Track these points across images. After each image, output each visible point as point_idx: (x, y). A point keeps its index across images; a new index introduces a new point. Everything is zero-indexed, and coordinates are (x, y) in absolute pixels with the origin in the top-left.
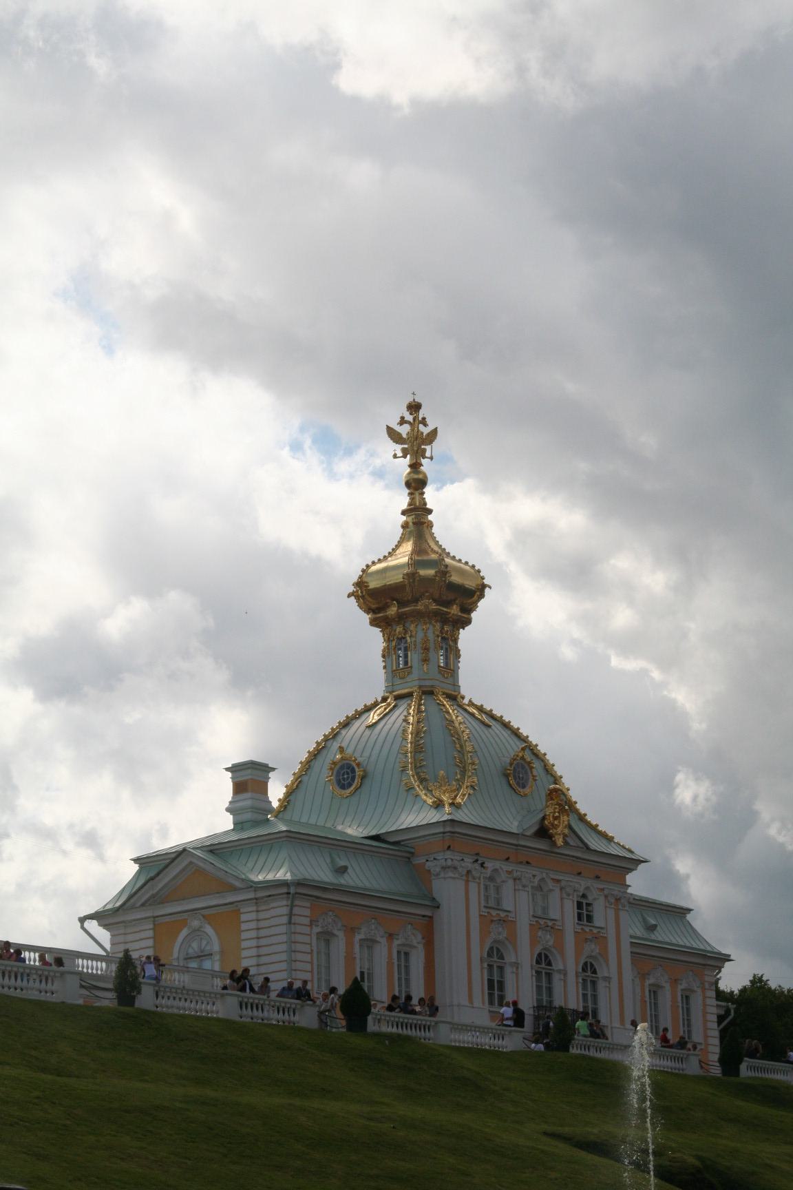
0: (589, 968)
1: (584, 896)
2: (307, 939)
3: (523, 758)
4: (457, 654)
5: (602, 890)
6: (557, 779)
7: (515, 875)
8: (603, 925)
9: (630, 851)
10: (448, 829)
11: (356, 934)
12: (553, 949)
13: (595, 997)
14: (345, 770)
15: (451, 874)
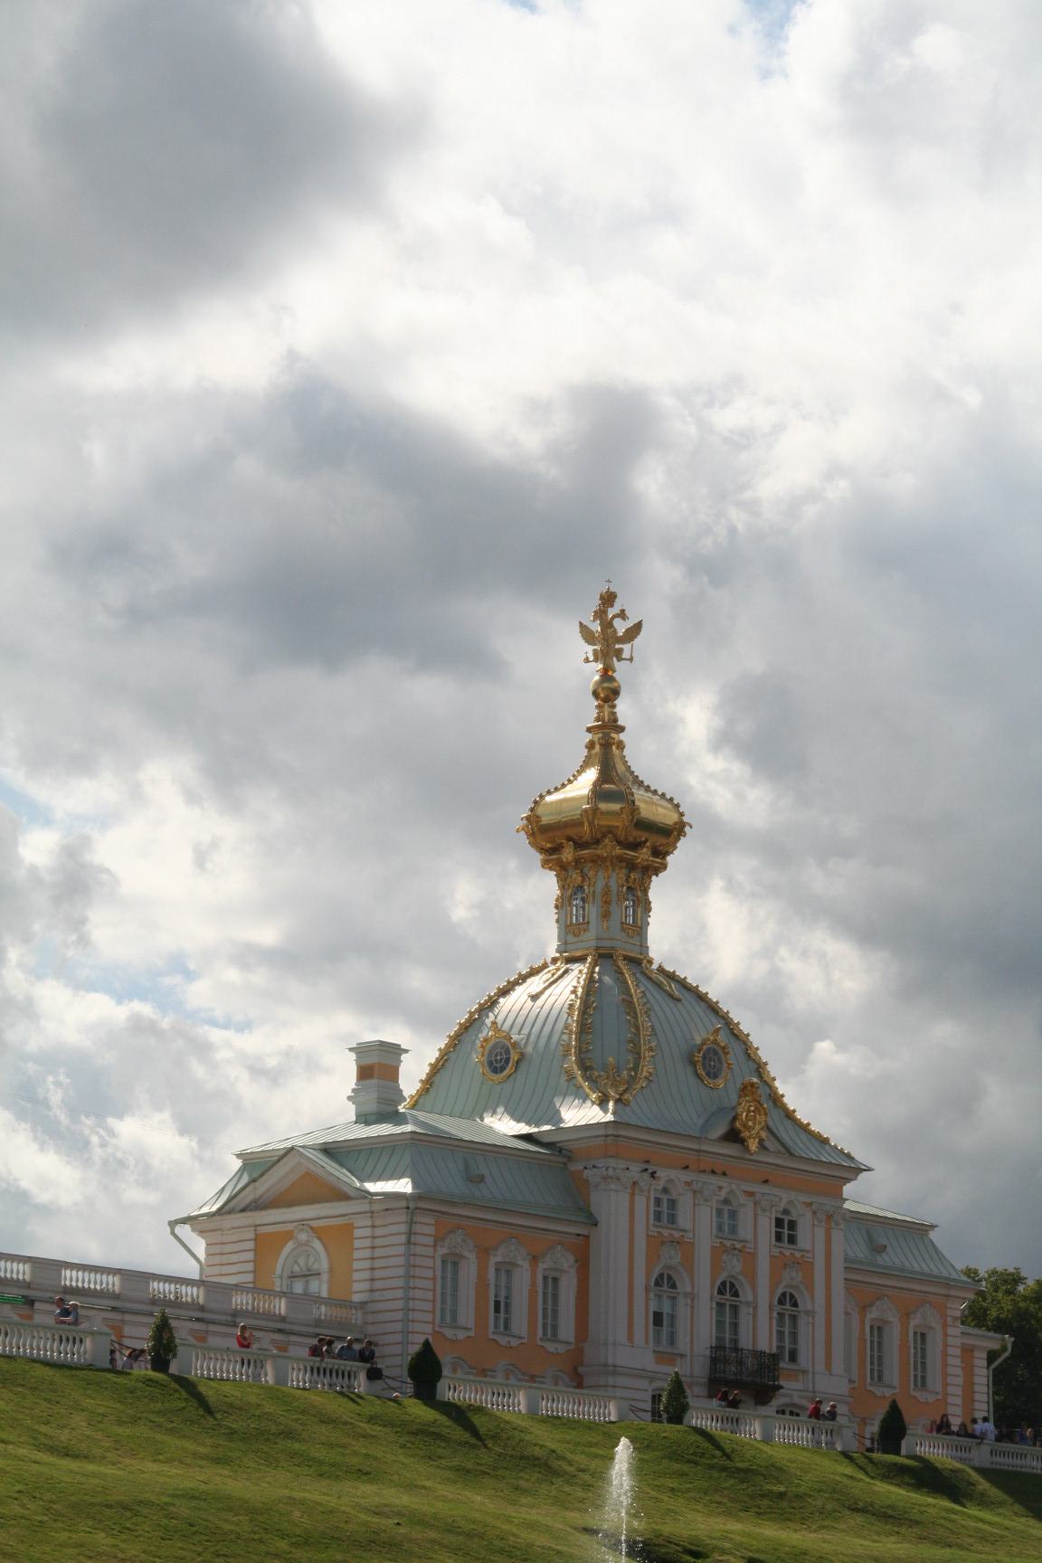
0: (788, 1299)
1: (786, 1212)
2: (429, 1262)
3: (715, 1042)
4: (647, 907)
5: (810, 1204)
6: (760, 1068)
7: (695, 1186)
8: (808, 1247)
9: (848, 1156)
10: (610, 1132)
11: (491, 1257)
12: (741, 1277)
13: (794, 1336)
14: (499, 1050)
15: (612, 1186)
